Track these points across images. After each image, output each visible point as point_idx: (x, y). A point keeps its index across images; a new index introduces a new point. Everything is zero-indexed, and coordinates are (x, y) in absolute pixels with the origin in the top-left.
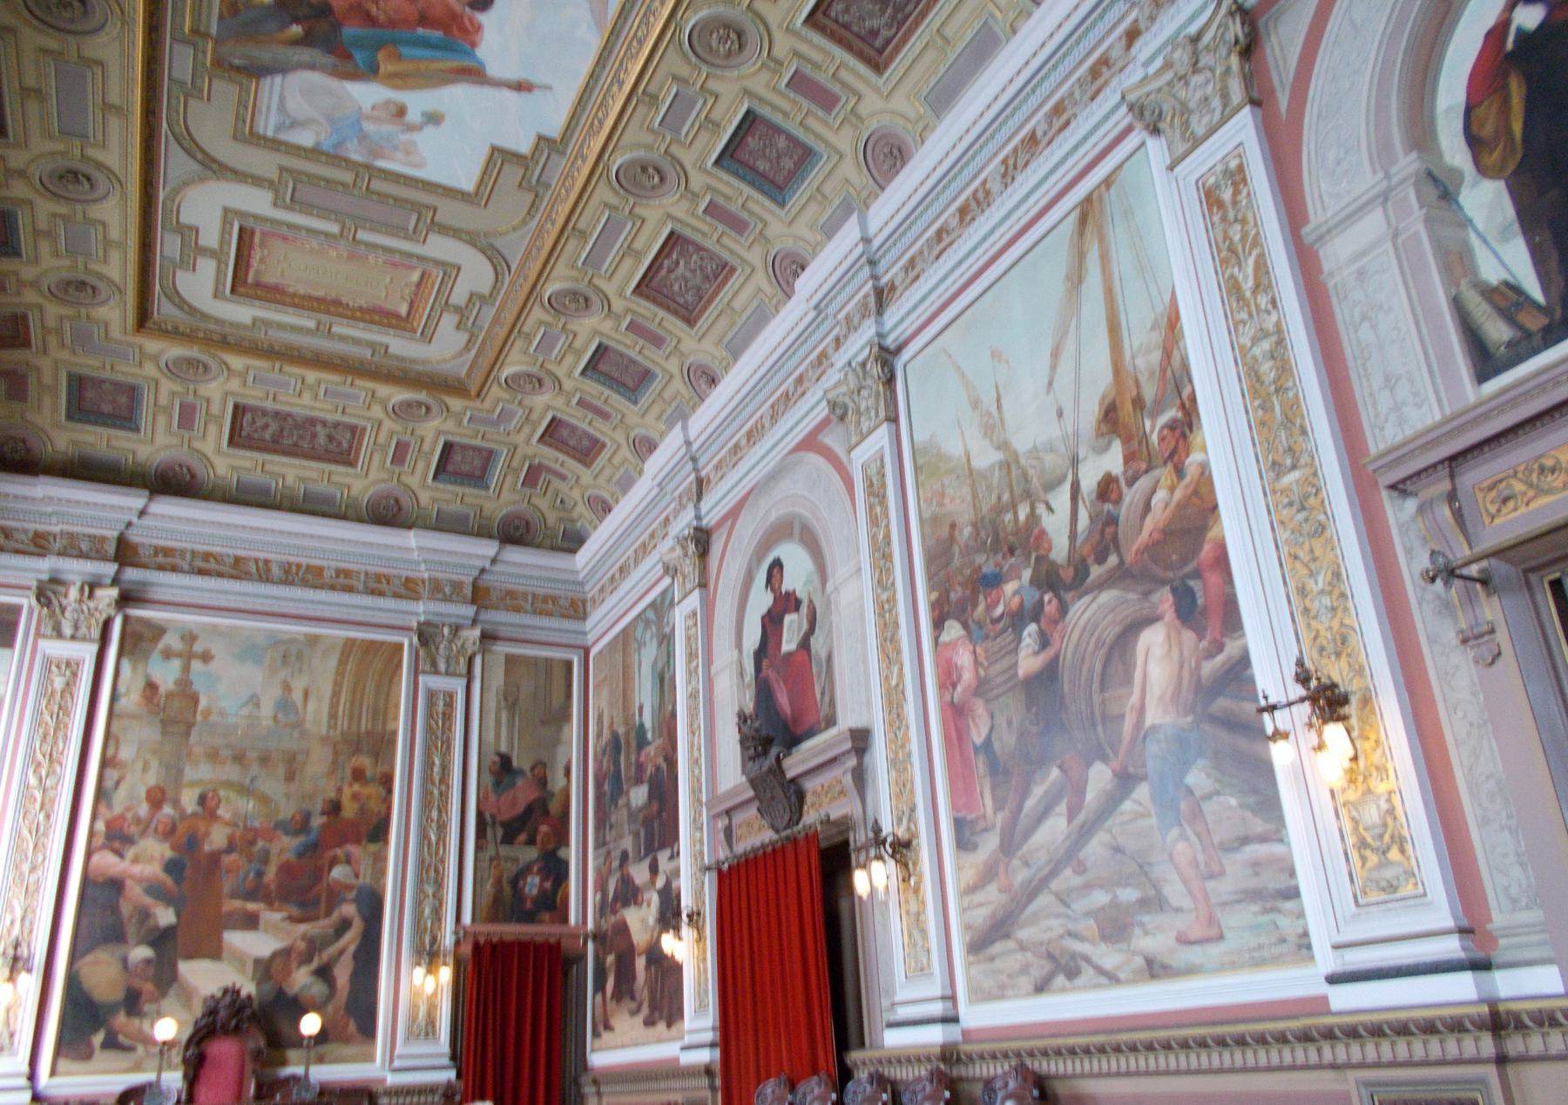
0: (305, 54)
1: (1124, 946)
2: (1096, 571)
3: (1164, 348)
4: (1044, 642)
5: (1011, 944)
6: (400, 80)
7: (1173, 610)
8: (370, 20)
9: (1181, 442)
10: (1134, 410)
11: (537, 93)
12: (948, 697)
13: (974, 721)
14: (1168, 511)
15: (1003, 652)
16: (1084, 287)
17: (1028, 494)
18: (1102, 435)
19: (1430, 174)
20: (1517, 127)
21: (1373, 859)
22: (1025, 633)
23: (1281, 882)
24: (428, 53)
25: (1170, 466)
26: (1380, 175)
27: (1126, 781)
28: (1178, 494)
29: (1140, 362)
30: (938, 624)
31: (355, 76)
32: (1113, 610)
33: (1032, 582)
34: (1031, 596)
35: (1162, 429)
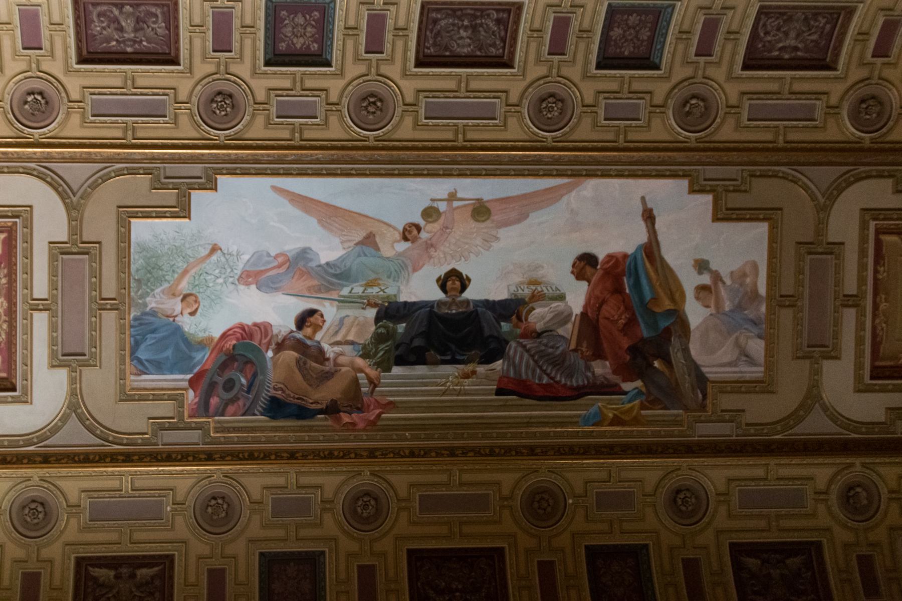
0: (677, 357)
6: (675, 292)
8: (632, 322)
11: (649, 206)
24: (644, 282)
31: (683, 324)
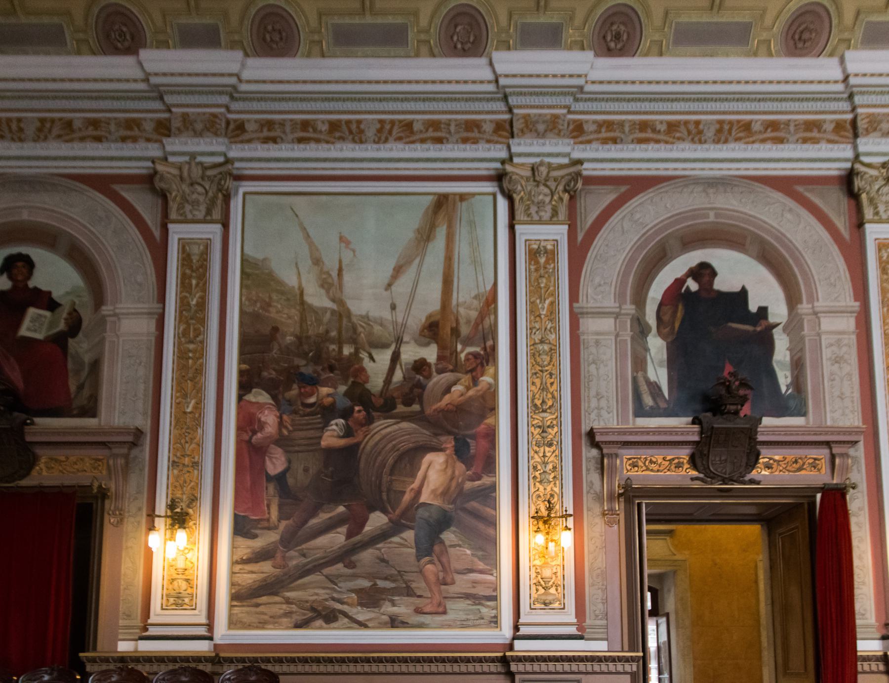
1: (376, 610)
2: (401, 408)
3: (480, 313)
4: (348, 433)
5: (277, 599)
7: (453, 449)
9: (479, 367)
10: (452, 335)
12: (246, 437)
13: (271, 458)
14: (461, 398)
15: (309, 427)
16: (431, 246)
17: (354, 341)
18: (424, 336)
19: (638, 319)
20: (677, 325)
21: (542, 591)
22: (333, 422)
23: (489, 592)
25: (469, 376)
26: (617, 305)
27: (396, 527)
28: (471, 393)
29: (462, 310)
30: (244, 387)
32: (409, 434)
33: (346, 394)
34: (343, 403)
35: (469, 354)
